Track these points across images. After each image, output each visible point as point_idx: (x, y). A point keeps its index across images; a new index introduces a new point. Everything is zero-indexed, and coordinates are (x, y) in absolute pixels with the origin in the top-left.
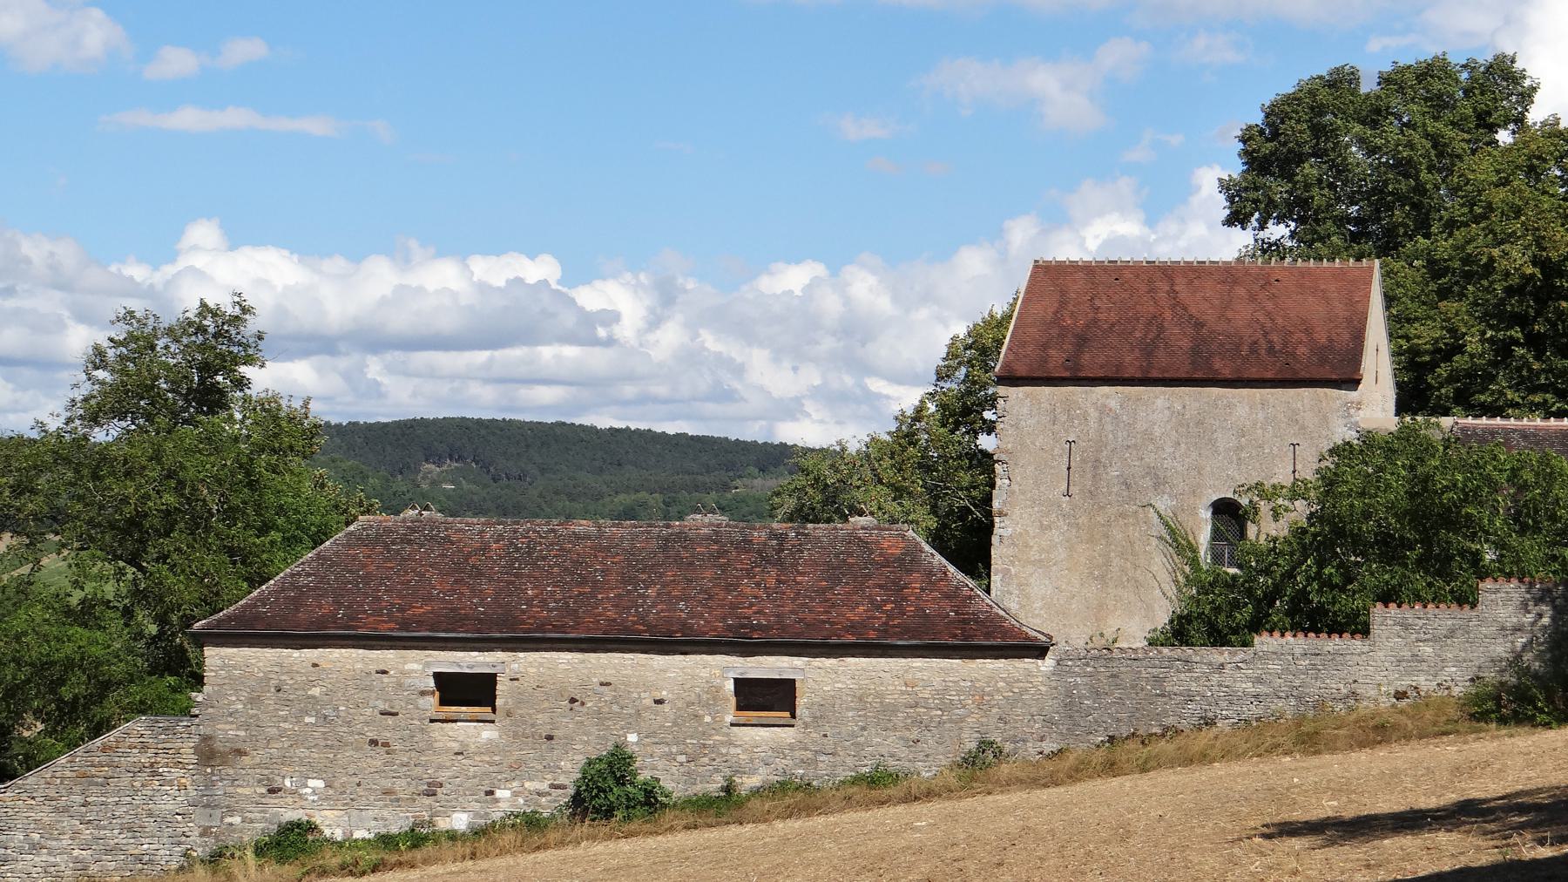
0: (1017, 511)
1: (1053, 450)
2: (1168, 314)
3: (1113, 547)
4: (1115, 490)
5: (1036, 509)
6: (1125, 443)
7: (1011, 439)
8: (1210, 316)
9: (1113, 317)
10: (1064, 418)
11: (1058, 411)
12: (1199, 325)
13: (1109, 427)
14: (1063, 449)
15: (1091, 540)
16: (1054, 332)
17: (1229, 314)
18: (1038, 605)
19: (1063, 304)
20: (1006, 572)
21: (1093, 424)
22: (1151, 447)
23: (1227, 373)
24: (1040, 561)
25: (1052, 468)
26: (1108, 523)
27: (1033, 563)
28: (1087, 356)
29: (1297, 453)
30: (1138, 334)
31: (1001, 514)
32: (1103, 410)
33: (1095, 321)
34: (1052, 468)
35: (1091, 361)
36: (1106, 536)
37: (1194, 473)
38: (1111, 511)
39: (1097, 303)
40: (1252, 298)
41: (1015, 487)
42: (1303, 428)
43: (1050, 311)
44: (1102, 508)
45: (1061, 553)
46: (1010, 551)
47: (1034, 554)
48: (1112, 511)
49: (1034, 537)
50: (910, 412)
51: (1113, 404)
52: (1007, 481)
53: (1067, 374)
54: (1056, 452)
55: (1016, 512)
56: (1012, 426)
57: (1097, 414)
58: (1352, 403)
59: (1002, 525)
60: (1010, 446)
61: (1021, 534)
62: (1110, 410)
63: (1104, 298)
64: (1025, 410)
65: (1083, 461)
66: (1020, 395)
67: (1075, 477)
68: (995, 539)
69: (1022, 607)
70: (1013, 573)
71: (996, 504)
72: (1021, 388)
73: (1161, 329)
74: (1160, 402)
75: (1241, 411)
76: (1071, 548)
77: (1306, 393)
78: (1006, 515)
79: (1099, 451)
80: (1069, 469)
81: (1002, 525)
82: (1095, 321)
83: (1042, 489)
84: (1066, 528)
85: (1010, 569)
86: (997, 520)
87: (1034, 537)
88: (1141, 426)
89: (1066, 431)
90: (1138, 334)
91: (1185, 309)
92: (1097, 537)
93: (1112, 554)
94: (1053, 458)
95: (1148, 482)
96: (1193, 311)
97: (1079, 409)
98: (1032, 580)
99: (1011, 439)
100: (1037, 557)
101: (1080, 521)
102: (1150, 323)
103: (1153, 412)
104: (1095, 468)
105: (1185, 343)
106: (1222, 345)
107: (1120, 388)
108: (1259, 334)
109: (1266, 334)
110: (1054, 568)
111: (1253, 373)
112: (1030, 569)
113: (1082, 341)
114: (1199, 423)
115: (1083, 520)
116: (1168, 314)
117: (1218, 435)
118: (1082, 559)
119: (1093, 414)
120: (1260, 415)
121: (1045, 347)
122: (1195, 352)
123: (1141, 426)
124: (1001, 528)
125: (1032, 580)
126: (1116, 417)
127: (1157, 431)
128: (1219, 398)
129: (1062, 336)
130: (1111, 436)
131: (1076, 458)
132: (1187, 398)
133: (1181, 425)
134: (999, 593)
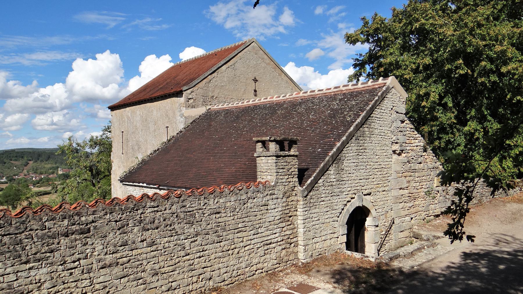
13: (129, 125)
37: (146, 143)
38: (130, 160)
42: (169, 119)
48: (130, 160)
58: (182, 104)
75: (155, 113)
77: (169, 100)
79: (128, 135)
95: (136, 148)
104: (127, 142)
114: (146, 120)
115: (125, 164)
117: (150, 125)
119: (126, 120)
123: (135, 124)
131: (124, 139)
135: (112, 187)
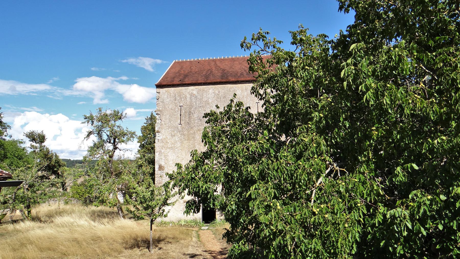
0: (163, 131)
1: (175, 109)
2: (214, 69)
3: (196, 141)
4: (196, 121)
5: (170, 129)
6: (199, 105)
7: (161, 106)
8: (227, 68)
9: (197, 70)
10: (178, 98)
11: (177, 96)
12: (224, 70)
13: (194, 100)
14: (178, 109)
15: (189, 139)
16: (178, 75)
17: (233, 67)
18: (171, 162)
19: (182, 68)
20: (160, 152)
21: (188, 99)
22: (208, 106)
23: (233, 79)
24: (171, 147)
25: (175, 115)
26: (194, 133)
27: (169, 148)
28: (187, 79)
29: (259, 105)
30: (204, 73)
31: (158, 132)
32: (192, 95)
33: (191, 72)
34: (175, 115)
35: (187, 81)
36: (194, 138)
39: (192, 68)
40: (240, 64)
41: (163, 123)
43: (177, 70)
44: (192, 128)
45: (178, 144)
46: (162, 144)
47: (169, 145)
48: (195, 129)
49: (169, 139)
50: (149, 116)
51: (195, 92)
52: (160, 121)
53: (179, 83)
54: (176, 110)
55: (163, 131)
56: (161, 102)
57: (190, 96)
59: (159, 135)
60: (161, 109)
61: (165, 139)
62: (194, 95)
63: (194, 67)
64: (166, 97)
65: (185, 112)
66: (164, 92)
67: (183, 118)
68: (156, 141)
69: (166, 163)
70: (162, 152)
71: (156, 129)
72: (164, 89)
73: (212, 72)
74: (211, 91)
76: (182, 143)
78: (160, 132)
79: (190, 109)
80: (181, 115)
81: (159, 135)
82: (191, 72)
83: (172, 122)
84: (180, 135)
85: (161, 151)
86: (157, 134)
87: (169, 139)
88: (205, 99)
89: (179, 103)
90: (204, 73)
91: (220, 67)
92: (191, 138)
93: (196, 144)
94: (175, 112)
96: (222, 67)
97: (184, 95)
98: (169, 154)
99: (161, 106)
100: (170, 146)
101: (185, 133)
102: (208, 71)
103: (209, 94)
104: (189, 114)
105: (219, 74)
106: (231, 74)
107: (197, 87)
108: (243, 71)
109: (245, 71)
110: (176, 150)
111: (243, 79)
112: (168, 150)
113: (186, 76)
115: (186, 132)
116: (214, 69)
118: (186, 146)
119: (188, 96)
120: (245, 93)
121: (174, 78)
122: (222, 76)
123: (205, 99)
124: (159, 137)
125: (169, 154)
126: (196, 97)
127: (210, 101)
128: (230, 88)
129: (180, 75)
130: (194, 103)
131: (183, 111)
132: (220, 89)
133: (218, 98)
134: (158, 159)
135: (157, 154)
